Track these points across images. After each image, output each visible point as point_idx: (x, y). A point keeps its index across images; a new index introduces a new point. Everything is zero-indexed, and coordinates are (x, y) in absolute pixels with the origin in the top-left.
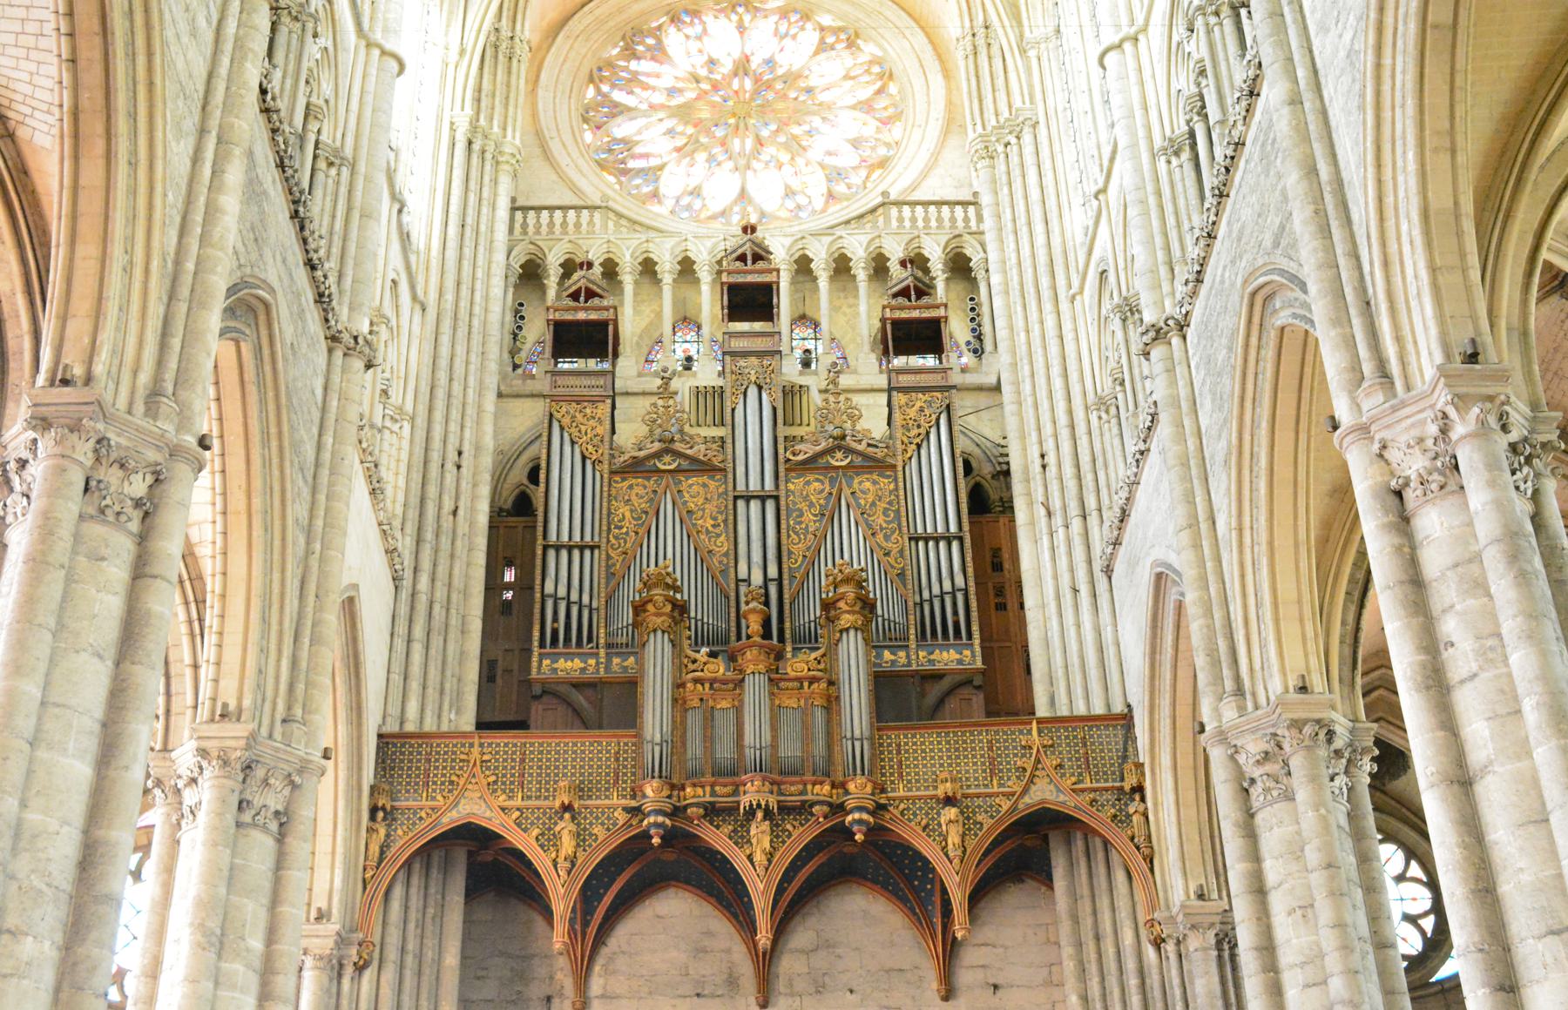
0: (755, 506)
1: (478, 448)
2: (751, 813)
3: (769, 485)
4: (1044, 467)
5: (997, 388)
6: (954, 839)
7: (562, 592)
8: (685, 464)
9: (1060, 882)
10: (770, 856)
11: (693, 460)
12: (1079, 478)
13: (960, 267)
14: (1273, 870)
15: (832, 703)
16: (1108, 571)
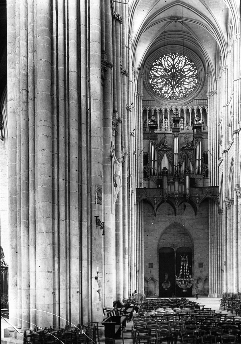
0: (176, 155)
1: (141, 146)
2: (175, 199)
3: (178, 152)
4: (212, 150)
5: (207, 133)
6: (198, 201)
7: (153, 167)
8: (167, 149)
9: (209, 205)
10: (178, 203)
11: (168, 148)
12: (216, 153)
13: (204, 110)
14: (228, 215)
15: (185, 184)
16: (219, 167)
